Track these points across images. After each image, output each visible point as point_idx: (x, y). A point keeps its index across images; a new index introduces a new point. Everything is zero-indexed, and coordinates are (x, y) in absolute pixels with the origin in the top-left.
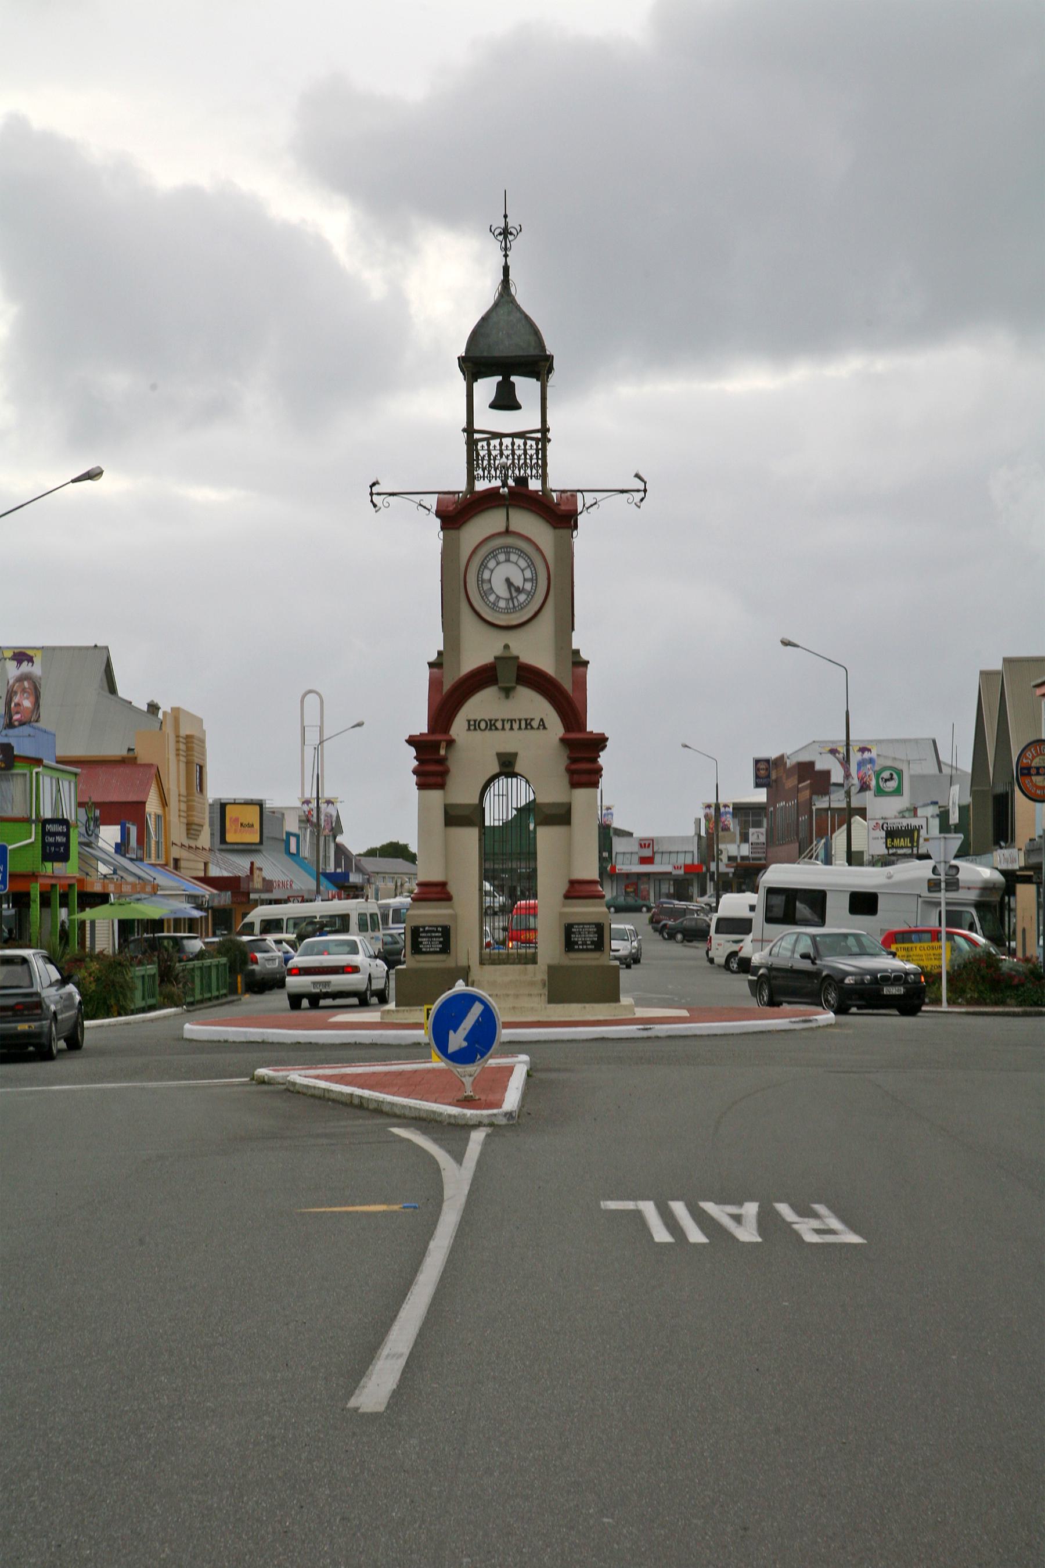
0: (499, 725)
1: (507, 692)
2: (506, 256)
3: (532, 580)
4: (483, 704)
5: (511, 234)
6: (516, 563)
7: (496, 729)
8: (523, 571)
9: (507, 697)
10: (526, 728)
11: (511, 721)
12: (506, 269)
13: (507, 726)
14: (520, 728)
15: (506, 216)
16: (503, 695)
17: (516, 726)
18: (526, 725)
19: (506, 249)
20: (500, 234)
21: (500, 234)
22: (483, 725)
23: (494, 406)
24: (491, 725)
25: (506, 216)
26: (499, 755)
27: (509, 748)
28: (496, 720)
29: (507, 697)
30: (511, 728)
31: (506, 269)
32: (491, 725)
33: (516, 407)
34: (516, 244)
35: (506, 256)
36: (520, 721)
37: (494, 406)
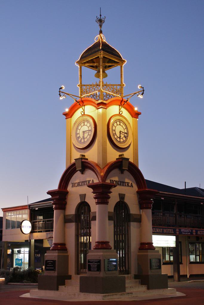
0: (81, 184)
1: (82, 172)
4: (78, 177)
15: (101, 15)
24: (79, 184)
25: (101, 15)
27: (83, 193)
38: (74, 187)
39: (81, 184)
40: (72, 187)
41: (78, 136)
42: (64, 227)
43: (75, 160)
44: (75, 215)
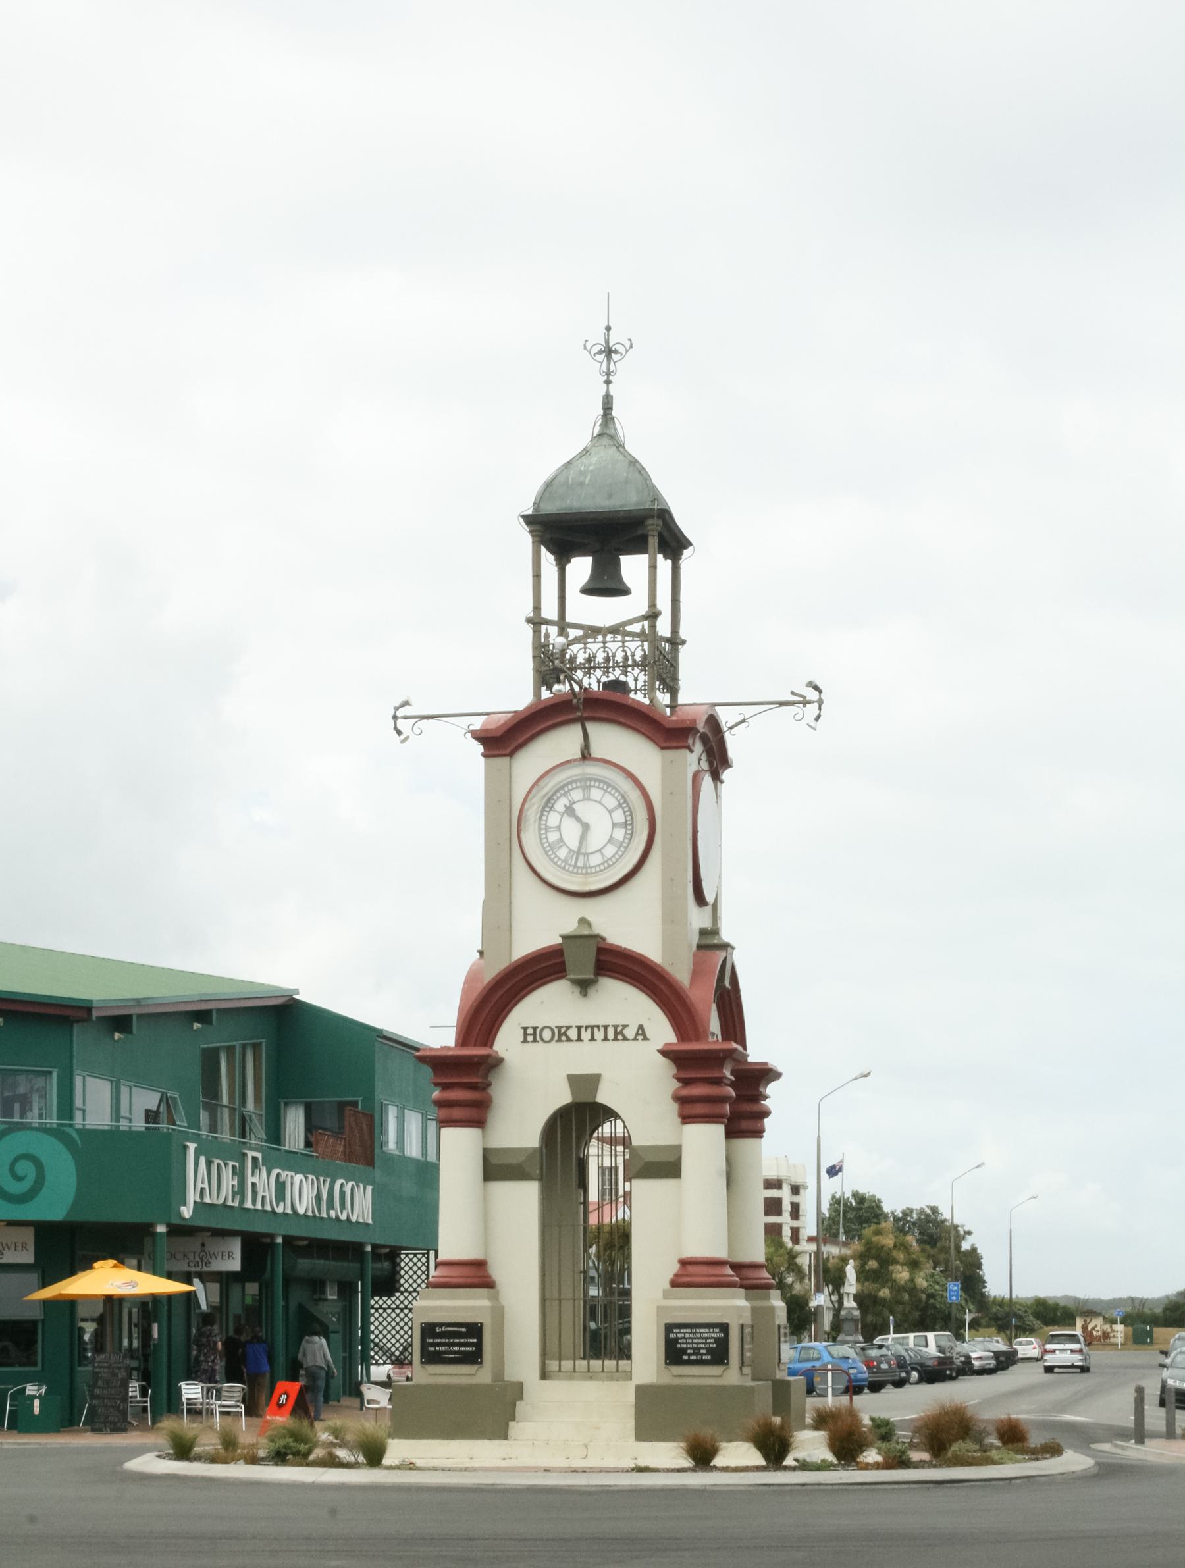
0: (573, 1033)
1: (584, 986)
2: (608, 382)
3: (625, 825)
5: (616, 352)
6: (599, 802)
7: (569, 1040)
8: (610, 812)
9: (584, 994)
10: (616, 1039)
11: (592, 1027)
12: (607, 404)
13: (586, 1035)
14: (606, 1039)
15: (608, 329)
16: (577, 990)
17: (599, 1035)
18: (616, 1034)
19: (608, 374)
20: (600, 352)
21: (600, 352)
22: (547, 1035)
23: (588, 590)
24: (561, 1034)
25: (608, 329)
26: (575, 1081)
28: (568, 1028)
29: (584, 994)
30: (592, 1039)
31: (607, 404)
32: (561, 1034)
33: (621, 590)
34: (622, 367)
35: (608, 382)
36: (606, 1027)
37: (588, 590)
38: (535, 1040)
39: (573, 1033)
40: (525, 1041)
41: (553, 837)
42: (485, 1200)
43: (564, 937)
44: (541, 1149)
